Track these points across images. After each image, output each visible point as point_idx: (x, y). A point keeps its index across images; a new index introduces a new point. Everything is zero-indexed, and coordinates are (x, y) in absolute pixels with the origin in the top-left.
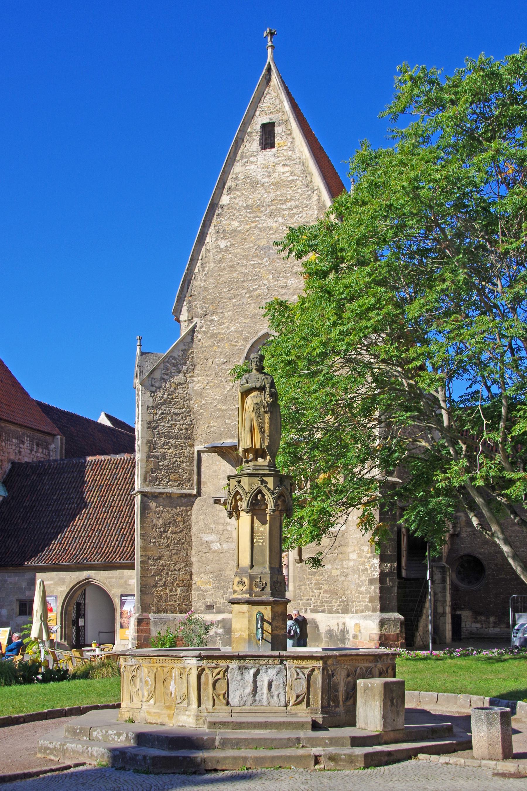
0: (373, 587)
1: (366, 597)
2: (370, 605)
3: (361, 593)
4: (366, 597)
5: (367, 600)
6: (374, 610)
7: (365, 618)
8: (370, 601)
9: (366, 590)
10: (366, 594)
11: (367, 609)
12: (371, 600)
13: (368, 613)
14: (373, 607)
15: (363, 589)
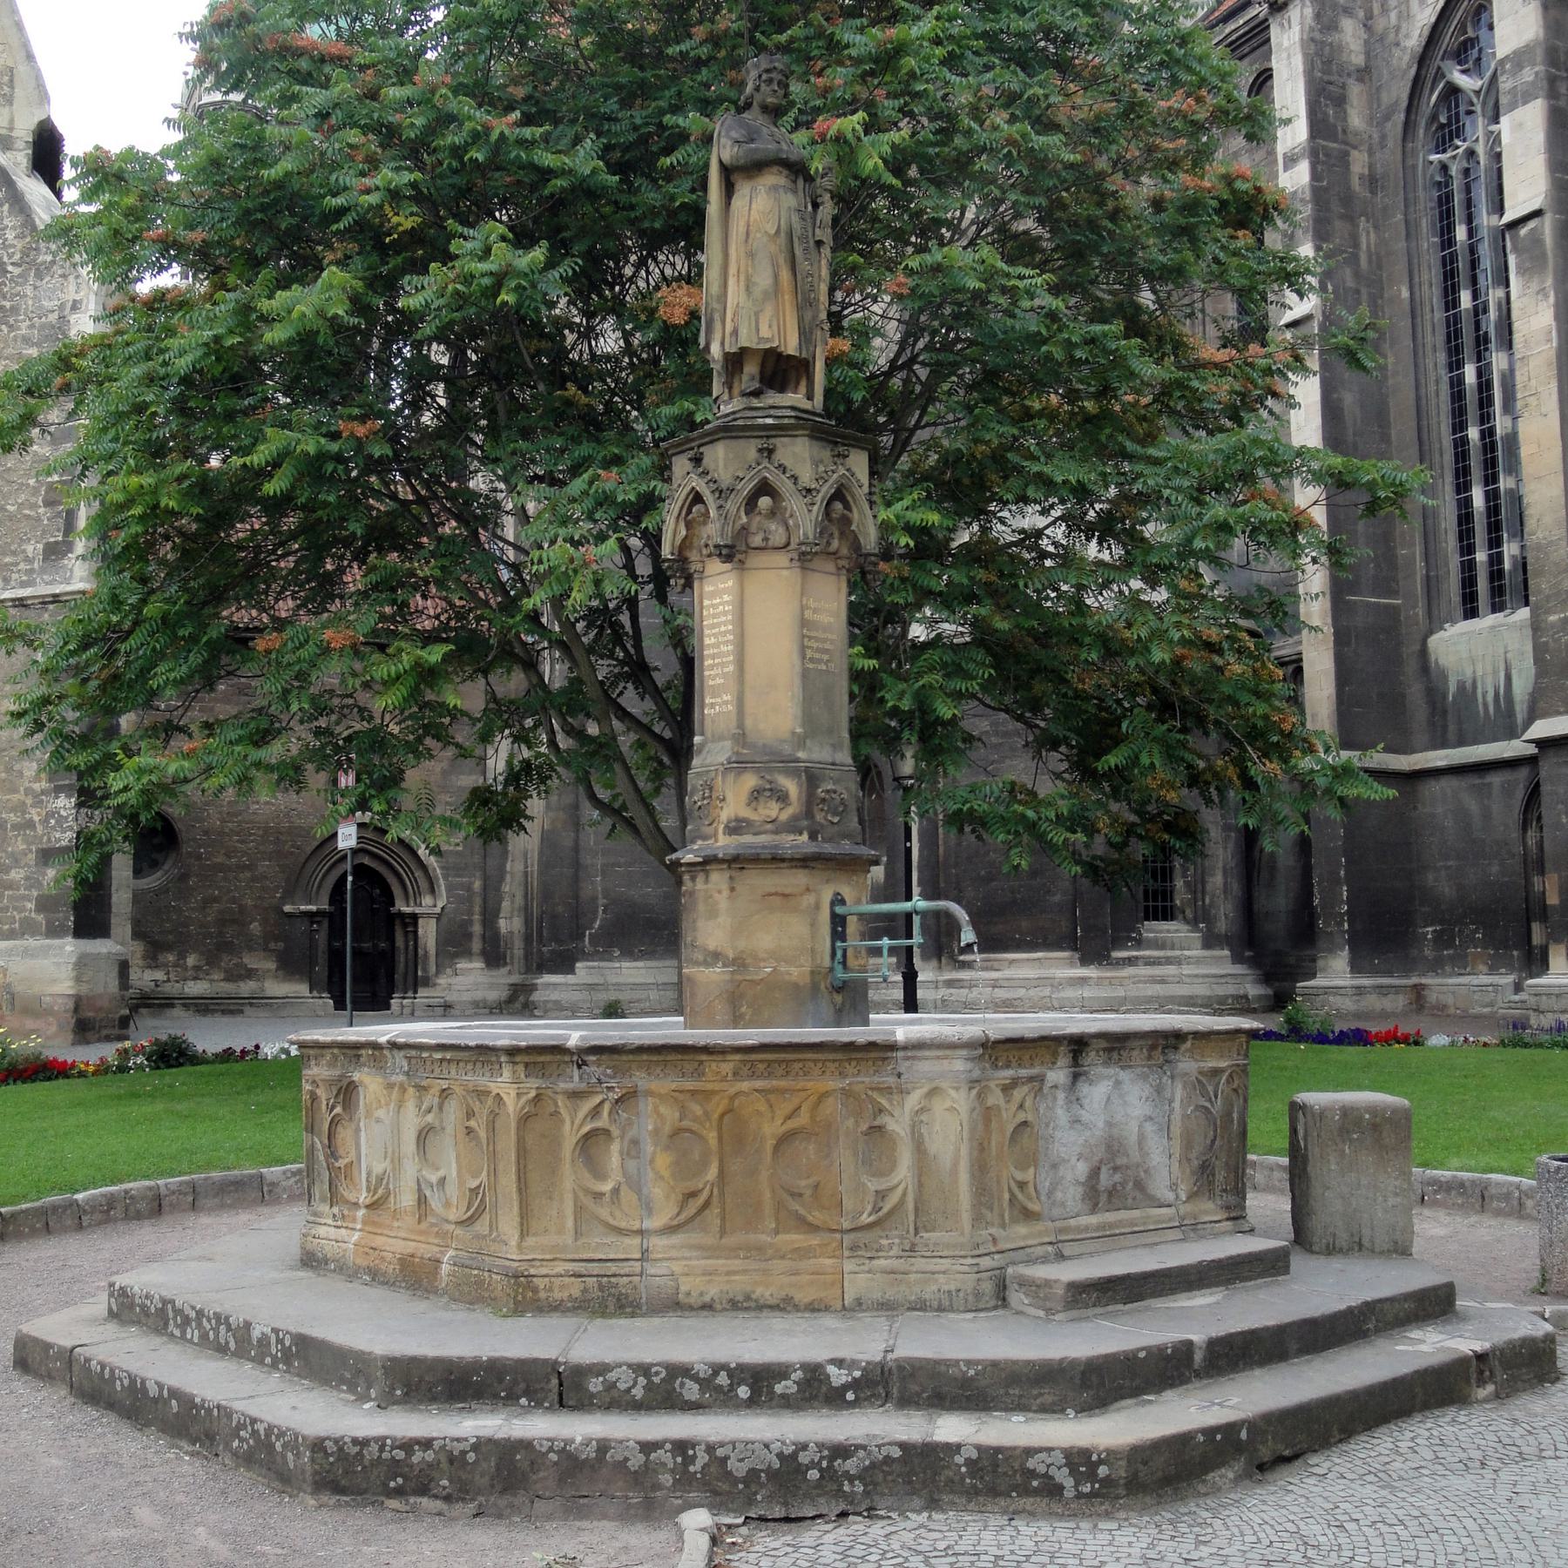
0: (51, 873)
1: (24, 898)
2: (40, 918)
3: (11, 886)
4: (24, 898)
5: (30, 905)
6: (53, 932)
7: (27, 953)
8: (39, 909)
9: (27, 878)
10: (27, 888)
11: (28, 928)
12: (44, 904)
13: (32, 942)
14: (49, 923)
15: (16, 875)
